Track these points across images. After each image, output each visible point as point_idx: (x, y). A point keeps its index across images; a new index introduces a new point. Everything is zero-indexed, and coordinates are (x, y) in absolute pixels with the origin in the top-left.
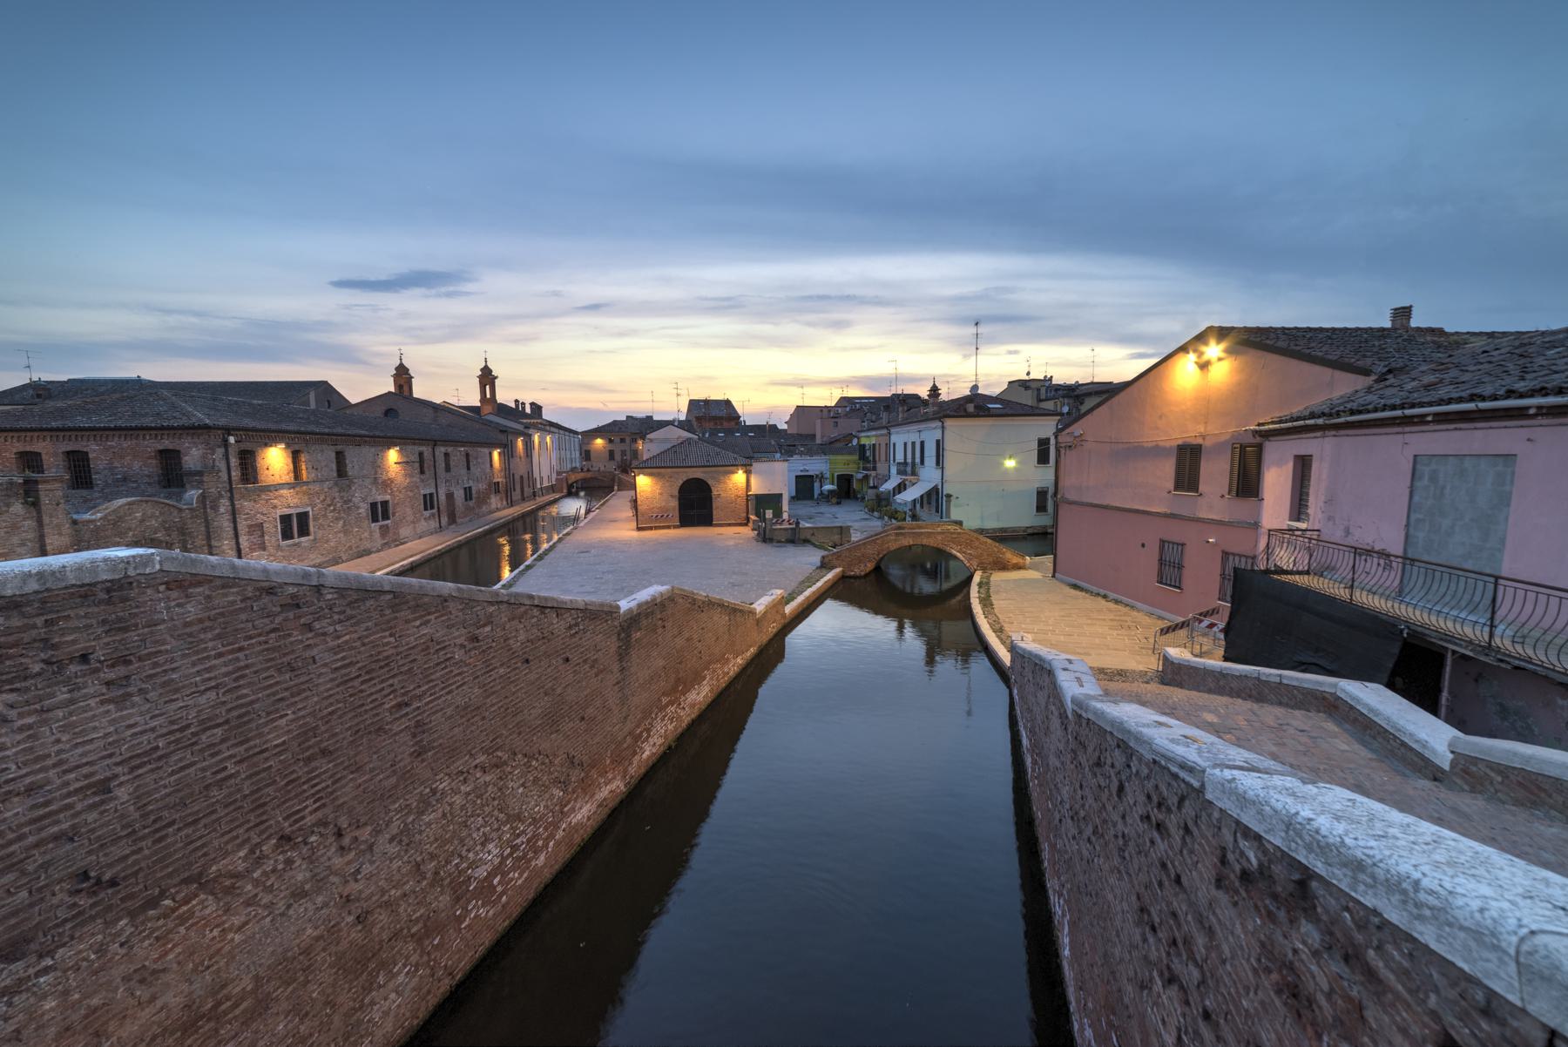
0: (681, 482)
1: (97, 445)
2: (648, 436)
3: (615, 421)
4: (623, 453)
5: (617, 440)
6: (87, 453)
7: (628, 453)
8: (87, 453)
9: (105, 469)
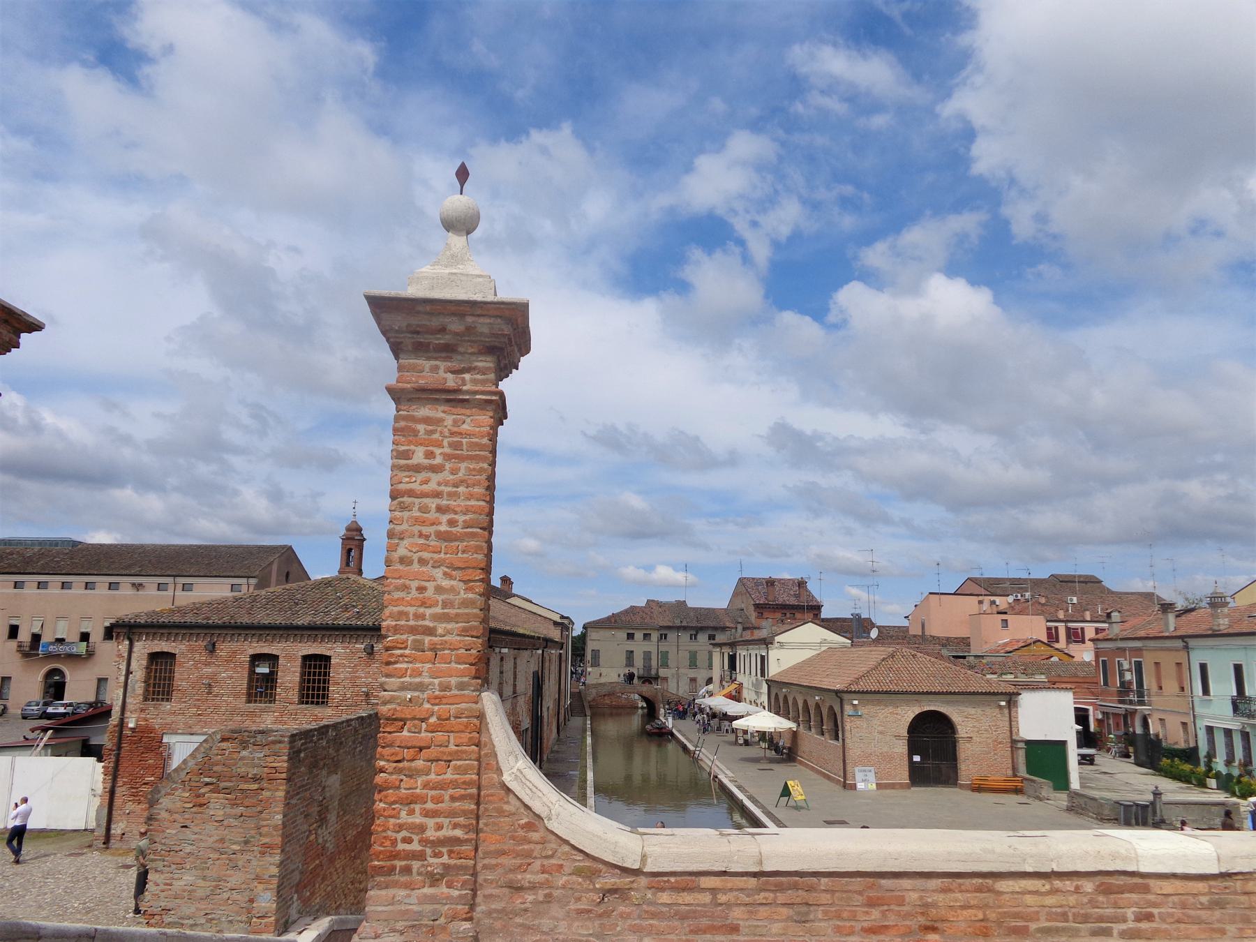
0: (912, 716)
1: (344, 648)
2: (777, 639)
3: (633, 608)
4: (647, 656)
5: (639, 635)
6: (328, 658)
7: (654, 657)
8: (328, 658)
9: (346, 678)
